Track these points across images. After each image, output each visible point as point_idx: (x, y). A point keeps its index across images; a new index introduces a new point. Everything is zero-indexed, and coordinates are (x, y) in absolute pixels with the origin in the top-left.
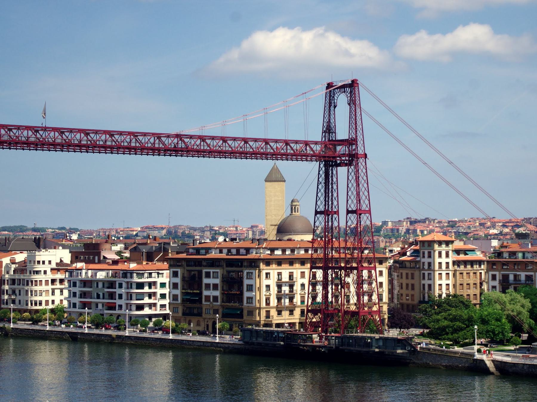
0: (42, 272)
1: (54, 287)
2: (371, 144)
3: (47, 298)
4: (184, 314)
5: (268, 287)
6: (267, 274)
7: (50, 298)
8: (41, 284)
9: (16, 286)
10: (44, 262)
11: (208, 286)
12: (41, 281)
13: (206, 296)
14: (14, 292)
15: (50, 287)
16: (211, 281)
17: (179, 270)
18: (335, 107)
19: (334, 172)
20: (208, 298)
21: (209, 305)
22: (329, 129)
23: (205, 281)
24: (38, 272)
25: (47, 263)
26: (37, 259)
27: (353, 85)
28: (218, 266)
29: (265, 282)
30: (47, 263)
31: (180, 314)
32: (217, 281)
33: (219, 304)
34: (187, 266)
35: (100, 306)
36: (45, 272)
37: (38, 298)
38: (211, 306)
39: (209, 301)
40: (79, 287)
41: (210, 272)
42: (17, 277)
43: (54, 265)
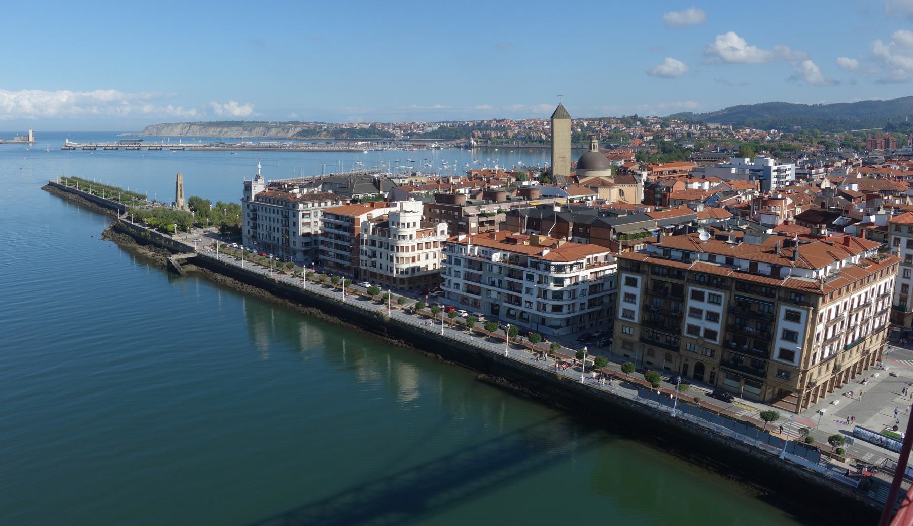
4: (642, 339)
8: (407, 251)
9: (376, 248)
11: (696, 313)
12: (407, 247)
14: (374, 255)
16: (705, 306)
17: (639, 279)
20: (694, 330)
21: (697, 340)
23: (691, 303)
24: (404, 237)
25: (411, 225)
26: (402, 221)
28: (726, 288)
30: (411, 225)
32: (718, 309)
33: (717, 343)
36: (411, 237)
38: (700, 342)
39: (698, 335)
41: (703, 293)
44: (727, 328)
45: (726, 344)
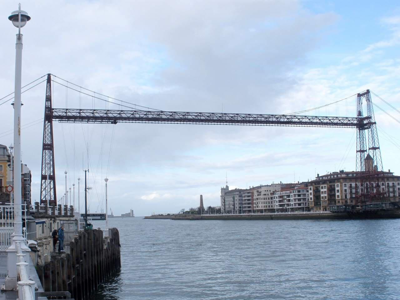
0: (267, 195)
1: (272, 200)
2: (377, 117)
3: (269, 205)
4: (314, 205)
5: (346, 190)
6: (345, 185)
7: (270, 205)
9: (258, 201)
10: (267, 191)
11: (322, 192)
12: (266, 198)
13: (322, 197)
15: (270, 200)
18: (362, 104)
19: (364, 133)
20: (323, 197)
22: (360, 113)
23: (322, 190)
25: (269, 191)
27: (368, 92)
29: (344, 188)
30: (269, 191)
31: (313, 206)
34: (315, 185)
35: (286, 206)
36: (268, 194)
37: (265, 205)
40: (278, 198)
41: (323, 186)
42: (258, 197)
43: (272, 192)
44: (328, 194)
45: (328, 200)
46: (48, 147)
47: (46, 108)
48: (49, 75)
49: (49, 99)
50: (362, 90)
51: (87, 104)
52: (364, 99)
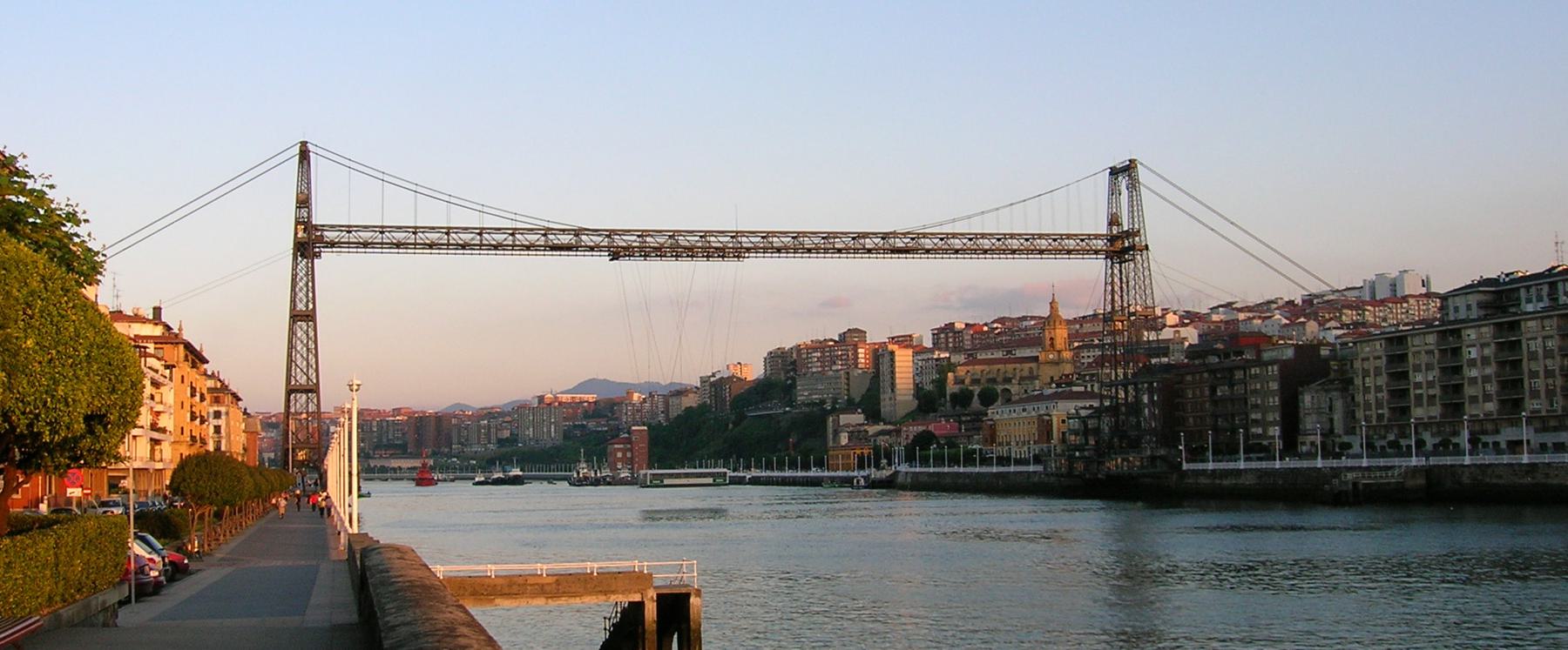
22: (1113, 221)
46: (302, 316)
47: (297, 223)
48: (304, 144)
49: (304, 202)
50: (1119, 160)
51: (400, 212)
52: (1123, 182)
